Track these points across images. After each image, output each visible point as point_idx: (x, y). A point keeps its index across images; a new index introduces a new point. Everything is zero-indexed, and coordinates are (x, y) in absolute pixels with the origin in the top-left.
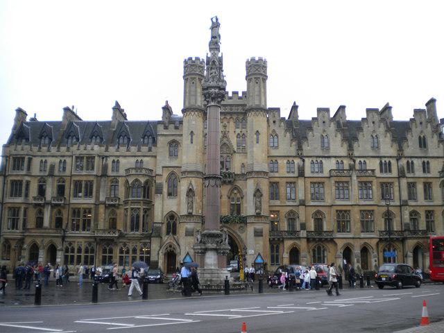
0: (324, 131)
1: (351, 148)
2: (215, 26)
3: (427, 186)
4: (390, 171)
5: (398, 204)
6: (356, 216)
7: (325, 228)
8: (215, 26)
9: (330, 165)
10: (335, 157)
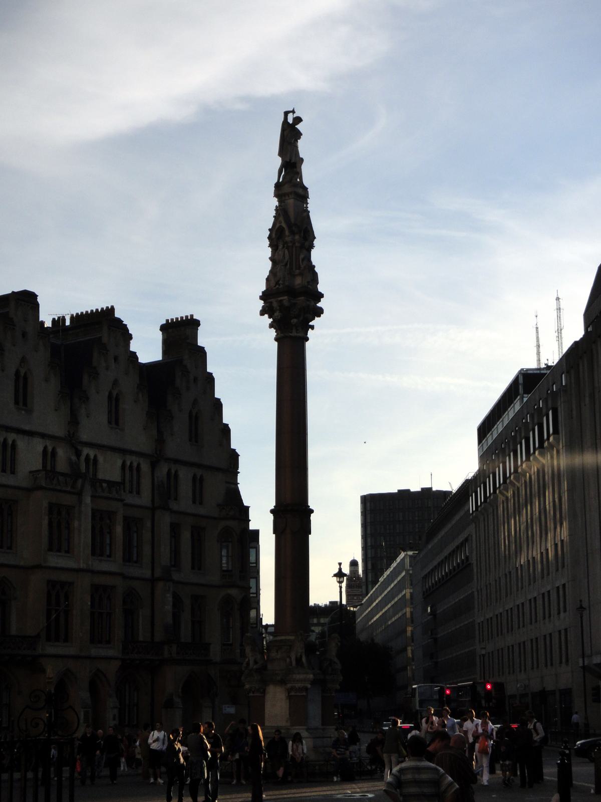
0: (23, 360)
1: (74, 421)
2: (290, 134)
3: (198, 534)
4: (138, 493)
5: (147, 573)
6: (81, 601)
7: (14, 631)
8: (290, 134)
9: (30, 455)
10: (43, 436)
